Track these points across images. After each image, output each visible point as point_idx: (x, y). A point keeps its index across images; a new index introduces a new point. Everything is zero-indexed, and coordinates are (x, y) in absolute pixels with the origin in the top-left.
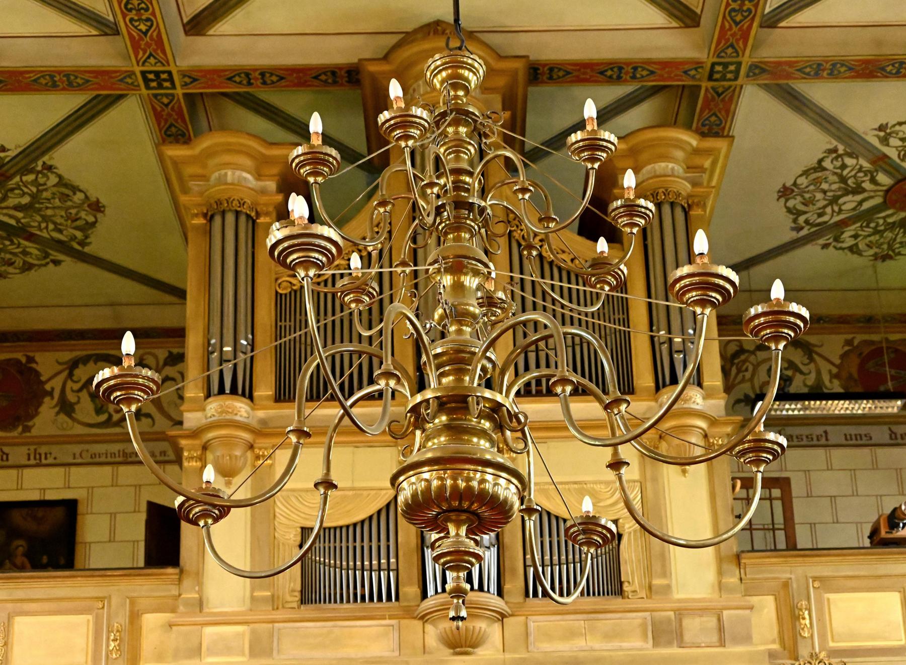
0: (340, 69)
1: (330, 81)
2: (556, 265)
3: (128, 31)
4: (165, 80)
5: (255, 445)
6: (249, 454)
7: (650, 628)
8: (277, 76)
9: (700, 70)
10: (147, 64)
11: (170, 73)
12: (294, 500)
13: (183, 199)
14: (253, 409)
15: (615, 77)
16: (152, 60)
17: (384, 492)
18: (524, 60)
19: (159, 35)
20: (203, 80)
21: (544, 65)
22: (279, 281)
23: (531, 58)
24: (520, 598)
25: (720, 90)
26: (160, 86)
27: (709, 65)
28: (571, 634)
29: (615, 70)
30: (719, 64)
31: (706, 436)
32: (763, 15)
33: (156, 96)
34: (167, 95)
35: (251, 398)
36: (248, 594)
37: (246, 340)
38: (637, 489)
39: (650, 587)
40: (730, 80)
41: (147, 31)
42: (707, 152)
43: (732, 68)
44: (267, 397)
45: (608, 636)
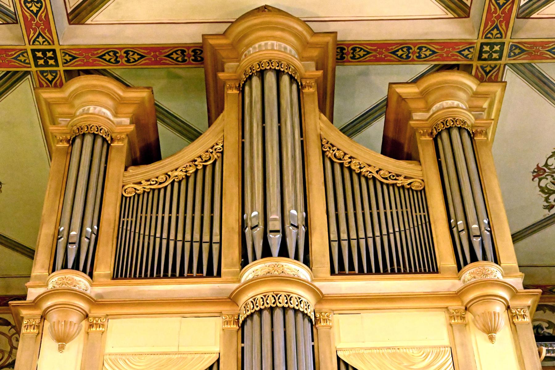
0: (188, 48)
1: (180, 59)
2: (364, 176)
3: (22, 10)
4: (51, 58)
5: (90, 315)
6: (84, 323)
8: (138, 54)
9: (471, 50)
10: (37, 43)
11: (54, 51)
12: (121, 362)
13: (51, 128)
14: (92, 285)
15: (404, 56)
16: (41, 39)
17: (208, 355)
18: (332, 35)
19: (47, 15)
20: (81, 58)
21: (348, 45)
22: (126, 187)
23: (339, 38)
25: (488, 69)
26: (46, 64)
27: (479, 45)
29: (405, 50)
30: (487, 44)
31: (508, 308)
32: (519, 8)
33: (42, 72)
34: (51, 72)
35: (91, 275)
37: (92, 228)
38: (448, 353)
40: (495, 59)
41: (38, 12)
42: (484, 96)
43: (497, 48)
44: (106, 276)
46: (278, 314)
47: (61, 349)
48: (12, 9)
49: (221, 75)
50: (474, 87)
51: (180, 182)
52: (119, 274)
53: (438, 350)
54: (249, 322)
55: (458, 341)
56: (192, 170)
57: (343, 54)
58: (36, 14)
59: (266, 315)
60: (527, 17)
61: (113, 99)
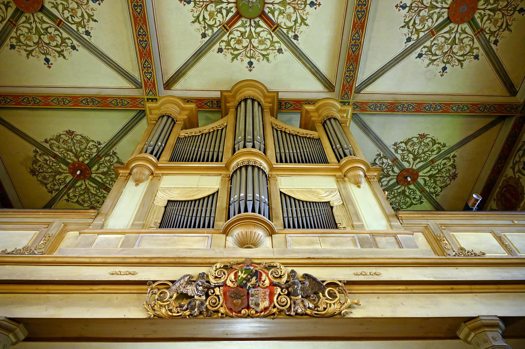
7: (357, 241)
24: (282, 228)
28: (312, 243)
36: (131, 223)
39: (353, 226)
45: (332, 244)
46: (250, 169)
47: (137, 185)
48: (140, 81)
49: (228, 104)
50: (340, 107)
51: (206, 134)
52: (171, 160)
53: (332, 191)
54: (235, 175)
55: (342, 186)
56: (212, 130)
58: (149, 79)
59: (243, 169)
61: (179, 107)
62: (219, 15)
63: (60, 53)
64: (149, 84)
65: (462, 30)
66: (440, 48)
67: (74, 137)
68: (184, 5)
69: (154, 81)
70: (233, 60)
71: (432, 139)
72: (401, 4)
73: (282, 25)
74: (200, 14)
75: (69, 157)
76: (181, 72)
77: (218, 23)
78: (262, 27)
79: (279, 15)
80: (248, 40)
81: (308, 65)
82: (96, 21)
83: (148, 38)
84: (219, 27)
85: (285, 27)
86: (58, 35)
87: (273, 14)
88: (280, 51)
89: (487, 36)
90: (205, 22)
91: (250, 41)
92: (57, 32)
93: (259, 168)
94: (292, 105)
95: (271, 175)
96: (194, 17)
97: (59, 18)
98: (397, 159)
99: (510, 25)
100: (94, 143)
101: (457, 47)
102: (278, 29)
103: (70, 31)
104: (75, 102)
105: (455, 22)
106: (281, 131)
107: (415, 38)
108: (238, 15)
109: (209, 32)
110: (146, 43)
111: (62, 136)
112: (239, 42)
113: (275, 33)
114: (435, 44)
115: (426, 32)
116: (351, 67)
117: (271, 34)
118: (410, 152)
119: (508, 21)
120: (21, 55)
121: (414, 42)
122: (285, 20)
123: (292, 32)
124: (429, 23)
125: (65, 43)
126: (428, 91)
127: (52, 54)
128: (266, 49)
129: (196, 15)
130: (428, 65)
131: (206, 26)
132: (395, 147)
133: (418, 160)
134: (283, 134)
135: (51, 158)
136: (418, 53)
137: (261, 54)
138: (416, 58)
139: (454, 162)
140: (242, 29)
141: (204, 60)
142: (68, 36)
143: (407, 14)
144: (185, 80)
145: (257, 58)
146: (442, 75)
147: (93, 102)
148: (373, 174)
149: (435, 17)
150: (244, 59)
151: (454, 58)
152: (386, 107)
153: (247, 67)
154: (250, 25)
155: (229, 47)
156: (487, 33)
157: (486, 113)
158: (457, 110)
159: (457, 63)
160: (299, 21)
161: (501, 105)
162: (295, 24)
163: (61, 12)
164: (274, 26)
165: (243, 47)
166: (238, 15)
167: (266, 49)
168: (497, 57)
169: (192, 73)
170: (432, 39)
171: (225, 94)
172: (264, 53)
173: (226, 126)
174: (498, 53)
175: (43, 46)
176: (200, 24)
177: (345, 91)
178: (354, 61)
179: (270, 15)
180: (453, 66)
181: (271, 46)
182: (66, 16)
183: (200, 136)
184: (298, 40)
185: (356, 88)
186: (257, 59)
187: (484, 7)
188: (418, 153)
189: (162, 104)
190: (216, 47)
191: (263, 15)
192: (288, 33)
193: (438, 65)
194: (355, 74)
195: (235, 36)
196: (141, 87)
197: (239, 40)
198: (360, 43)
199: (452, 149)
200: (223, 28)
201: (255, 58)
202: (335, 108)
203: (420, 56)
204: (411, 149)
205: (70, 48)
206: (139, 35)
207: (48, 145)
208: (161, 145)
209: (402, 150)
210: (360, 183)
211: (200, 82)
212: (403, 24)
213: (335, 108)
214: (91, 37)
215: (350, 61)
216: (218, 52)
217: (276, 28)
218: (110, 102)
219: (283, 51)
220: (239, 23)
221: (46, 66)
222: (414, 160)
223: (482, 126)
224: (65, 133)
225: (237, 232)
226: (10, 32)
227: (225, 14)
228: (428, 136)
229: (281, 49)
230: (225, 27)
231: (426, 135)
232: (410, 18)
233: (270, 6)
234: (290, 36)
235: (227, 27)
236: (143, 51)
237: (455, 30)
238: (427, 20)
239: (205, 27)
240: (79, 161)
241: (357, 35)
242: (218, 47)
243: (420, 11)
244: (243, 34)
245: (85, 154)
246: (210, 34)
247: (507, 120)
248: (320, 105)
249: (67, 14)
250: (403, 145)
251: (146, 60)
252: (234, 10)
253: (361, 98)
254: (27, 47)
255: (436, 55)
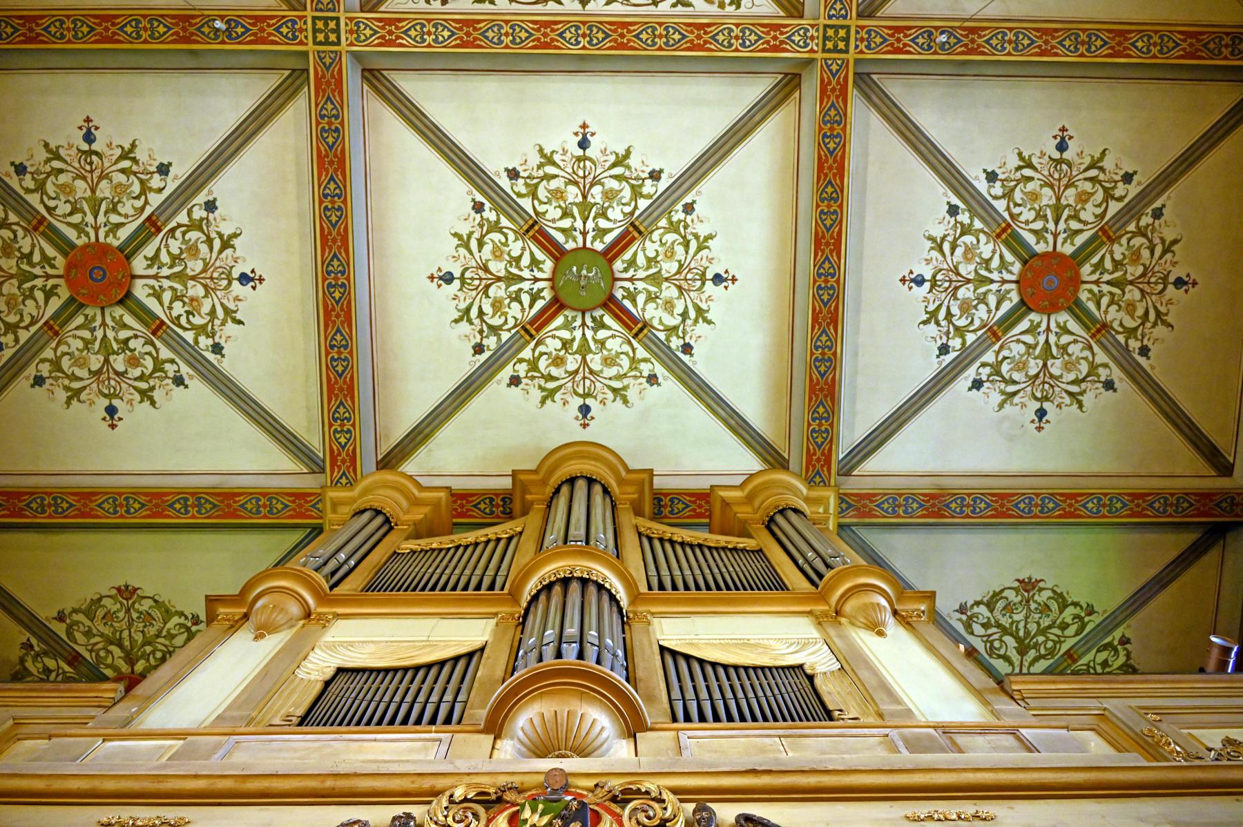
48: (321, 455)
49: (528, 497)
50: (805, 491)
51: (466, 547)
56: (483, 539)
57: (661, 506)
58: (343, 448)
60: (848, 474)
61: (407, 498)
62: (515, 305)
63: (146, 395)
64: (341, 462)
65: (1058, 325)
66: (1021, 366)
67: (134, 603)
68: (439, 286)
69: (354, 450)
70: (543, 402)
71: (1054, 592)
72: (913, 276)
73: (655, 323)
74: (471, 305)
75: (109, 661)
76: (420, 433)
77: (511, 322)
78: (609, 328)
79: (646, 303)
80: (579, 357)
81: (719, 410)
82: (240, 322)
83: (351, 353)
84: (513, 331)
85: (661, 328)
86: (149, 354)
87: (634, 301)
88: (652, 379)
89: (1121, 338)
90: (483, 321)
91: (584, 359)
92: (149, 348)
93: (600, 587)
94: (688, 506)
95: (635, 613)
96: (459, 311)
97: (158, 318)
98: (975, 650)
99: (1166, 314)
100: (182, 620)
101: (1058, 362)
102: (645, 331)
103: (178, 345)
104: (157, 506)
105: (1040, 311)
106: (661, 540)
107: (958, 346)
108: (557, 305)
109: (491, 342)
110: (345, 364)
111: (105, 602)
112: (558, 361)
113: (640, 341)
114: (1005, 358)
115: (980, 333)
116: (821, 410)
117: (630, 343)
118: (1005, 631)
119: (1158, 305)
120: (53, 400)
121: (956, 354)
122: (660, 313)
123: (678, 337)
124: (981, 313)
125: (162, 370)
126: (1015, 466)
127: (127, 397)
128: (619, 377)
129: (463, 306)
130: (1001, 406)
131: (485, 328)
132: (964, 617)
133: (1032, 654)
134: (668, 546)
135: (62, 664)
136: (971, 379)
137: (609, 387)
138: (970, 389)
139: (1128, 655)
140: (566, 334)
141: (478, 404)
142: (172, 356)
143: (929, 296)
144: (430, 450)
145: (600, 397)
146: (1039, 429)
147: (200, 506)
148: (916, 606)
149: (992, 300)
150: (569, 398)
151: (1056, 389)
152: (921, 506)
153: (577, 418)
154: (584, 324)
155: (536, 374)
156: (1118, 333)
157: (1170, 516)
158: (1099, 511)
159: (1067, 400)
160: (692, 314)
161: (1205, 496)
162: (684, 321)
163: (166, 304)
164: (636, 327)
165: (566, 372)
166: (557, 305)
167: (619, 377)
168: (1157, 384)
169: (447, 432)
170: (996, 347)
171: (522, 477)
172: (617, 384)
173: (521, 533)
174: (1156, 375)
175: (109, 379)
176: (472, 323)
177: (814, 466)
178: (826, 396)
179: (627, 304)
180: (1059, 406)
181: (631, 369)
182: (175, 314)
183: (452, 551)
184: (692, 355)
185: (839, 462)
186: (599, 398)
187: (1095, 277)
188: (1027, 632)
189: (365, 492)
190: (507, 373)
191: (610, 303)
192: (668, 339)
193: (1023, 405)
194: (832, 425)
195: (551, 349)
196: (323, 471)
197: (557, 357)
198: (835, 354)
199: (1112, 621)
200: (522, 332)
201: (595, 398)
202: (793, 487)
203: (977, 384)
204: (1005, 621)
205: (170, 381)
206: (332, 347)
207: (64, 626)
208: (346, 561)
209: (983, 625)
210: (883, 624)
211: (464, 455)
212: (925, 317)
213: (793, 487)
214: (223, 356)
215: (817, 396)
216: (509, 385)
217: (641, 330)
218: (242, 506)
219: (660, 380)
220: (559, 320)
221: (105, 424)
222: (1022, 652)
223: (1174, 554)
224: (114, 592)
225: (526, 718)
226: (42, 349)
227: (526, 305)
228: (1041, 585)
229: (655, 376)
230: (527, 331)
231: (1038, 581)
232: (937, 303)
233: (627, 284)
234: (673, 346)
235: (532, 329)
236: (336, 382)
237: (1044, 326)
238: (975, 307)
239: (481, 332)
240: (133, 672)
241: (824, 338)
242: (511, 373)
243: (957, 288)
244: (566, 344)
245: (153, 652)
246: (493, 346)
247: (1230, 537)
248: (755, 488)
249: (178, 308)
250: (982, 609)
251: (341, 403)
252: (547, 295)
253: (853, 485)
254: (71, 381)
255: (1015, 382)
